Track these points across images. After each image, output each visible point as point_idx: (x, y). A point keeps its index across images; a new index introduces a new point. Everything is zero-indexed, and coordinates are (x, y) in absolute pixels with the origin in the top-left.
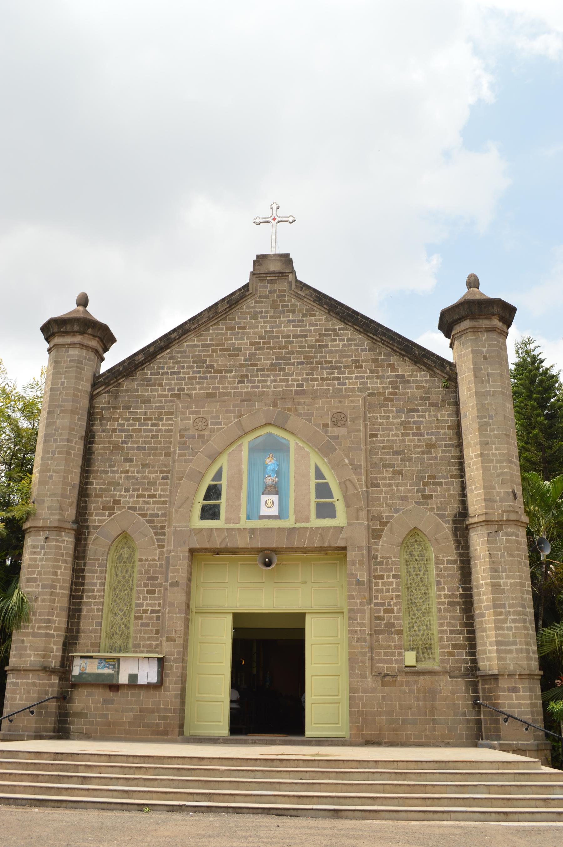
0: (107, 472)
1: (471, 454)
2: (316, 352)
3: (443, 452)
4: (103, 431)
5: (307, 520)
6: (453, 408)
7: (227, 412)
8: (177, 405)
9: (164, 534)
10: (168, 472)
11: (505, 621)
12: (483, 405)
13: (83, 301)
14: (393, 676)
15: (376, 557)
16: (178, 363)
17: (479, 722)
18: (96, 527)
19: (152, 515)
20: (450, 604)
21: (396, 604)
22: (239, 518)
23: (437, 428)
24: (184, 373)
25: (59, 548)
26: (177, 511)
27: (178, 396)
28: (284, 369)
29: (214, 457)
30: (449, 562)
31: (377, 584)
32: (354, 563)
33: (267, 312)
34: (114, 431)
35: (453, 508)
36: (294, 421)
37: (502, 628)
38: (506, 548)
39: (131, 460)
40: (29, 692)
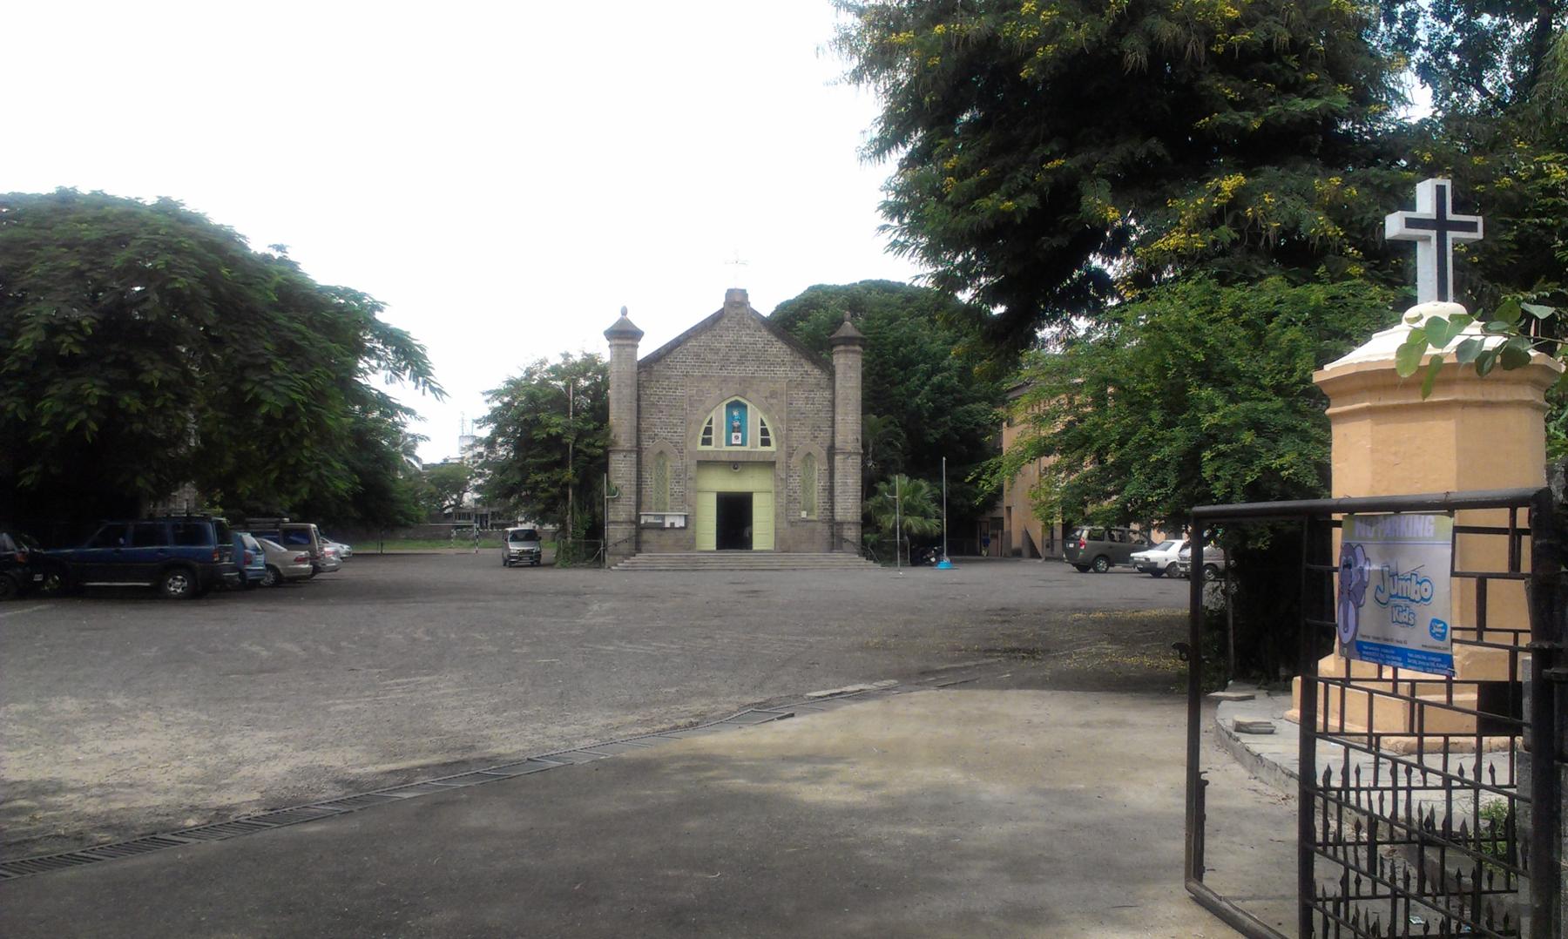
1: (838, 418)
13: (624, 312)
29: (708, 411)
35: (827, 444)
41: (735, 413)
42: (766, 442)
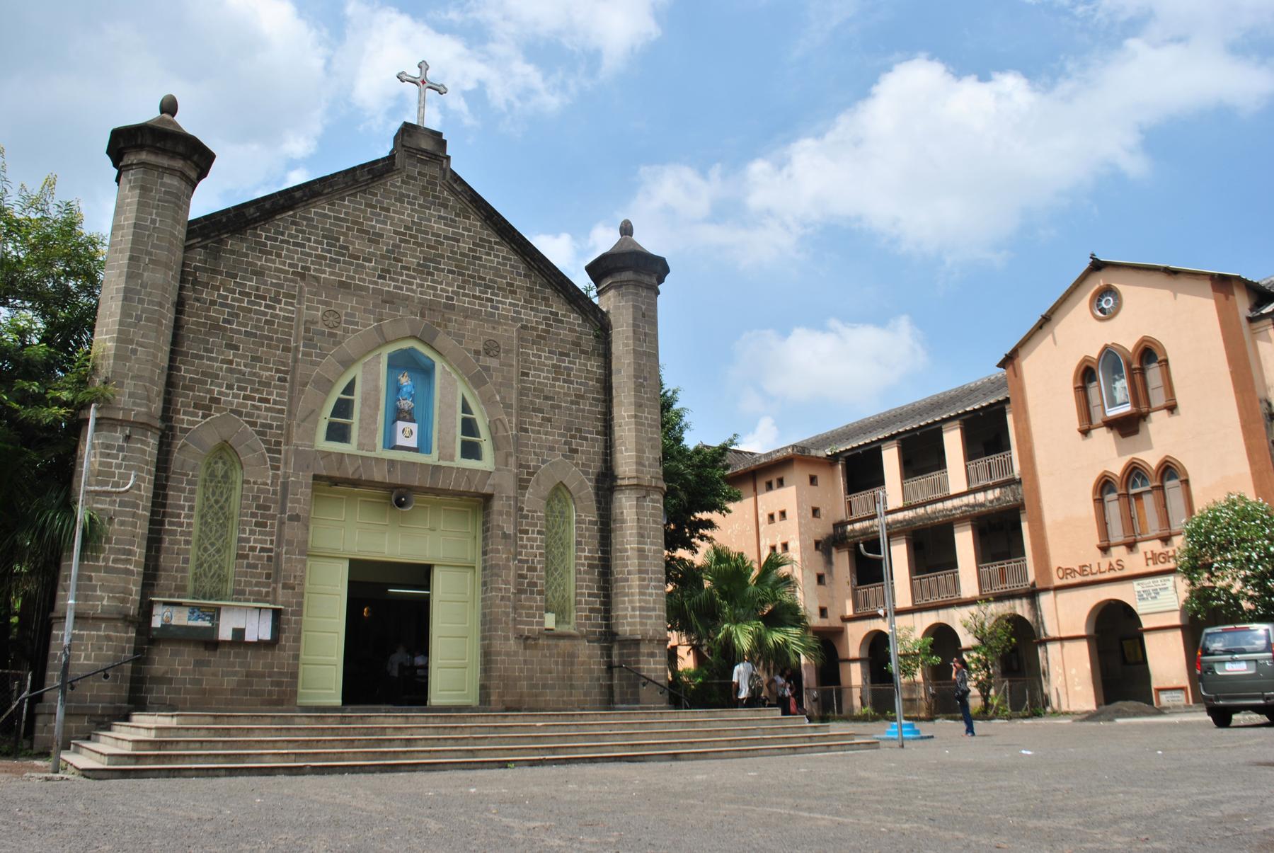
0: (201, 358)
2: (469, 263)
3: (591, 405)
4: (197, 300)
5: (452, 458)
6: (601, 359)
7: (366, 311)
8: (301, 288)
9: (279, 452)
10: (286, 372)
11: (647, 587)
12: (639, 365)
13: (169, 107)
14: (535, 639)
15: (521, 509)
16: (303, 232)
17: (610, 687)
18: (186, 431)
19: (263, 425)
20: (590, 566)
21: (539, 562)
22: (375, 446)
23: (586, 378)
24: (310, 247)
25: (144, 452)
26: (299, 425)
27: (302, 276)
28: (432, 274)
29: (347, 363)
30: (590, 522)
31: (521, 539)
32: (501, 513)
33: (415, 198)
34: (213, 303)
35: (596, 467)
36: (442, 340)
37: (644, 594)
38: (652, 515)
39: (236, 348)
40: (100, 649)
41: (405, 380)
42: (471, 450)
